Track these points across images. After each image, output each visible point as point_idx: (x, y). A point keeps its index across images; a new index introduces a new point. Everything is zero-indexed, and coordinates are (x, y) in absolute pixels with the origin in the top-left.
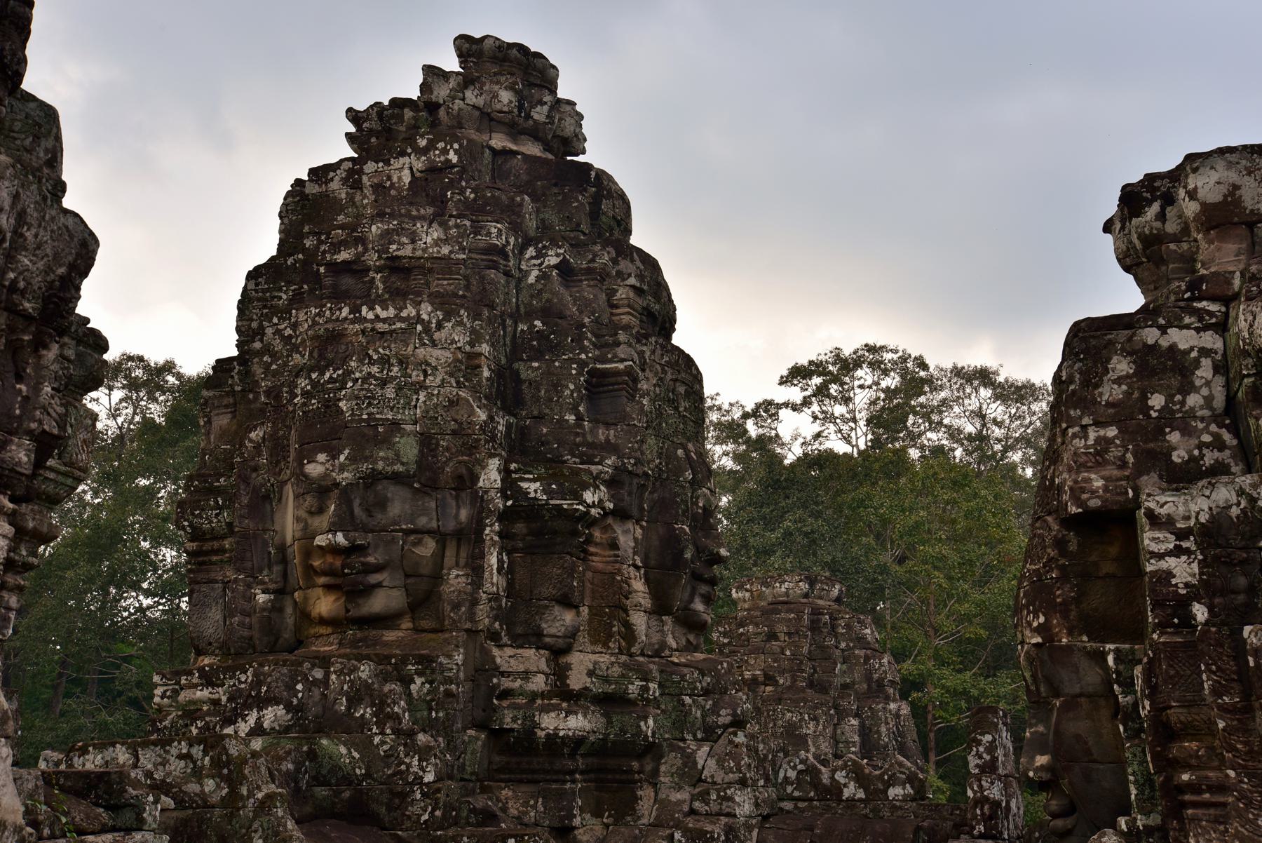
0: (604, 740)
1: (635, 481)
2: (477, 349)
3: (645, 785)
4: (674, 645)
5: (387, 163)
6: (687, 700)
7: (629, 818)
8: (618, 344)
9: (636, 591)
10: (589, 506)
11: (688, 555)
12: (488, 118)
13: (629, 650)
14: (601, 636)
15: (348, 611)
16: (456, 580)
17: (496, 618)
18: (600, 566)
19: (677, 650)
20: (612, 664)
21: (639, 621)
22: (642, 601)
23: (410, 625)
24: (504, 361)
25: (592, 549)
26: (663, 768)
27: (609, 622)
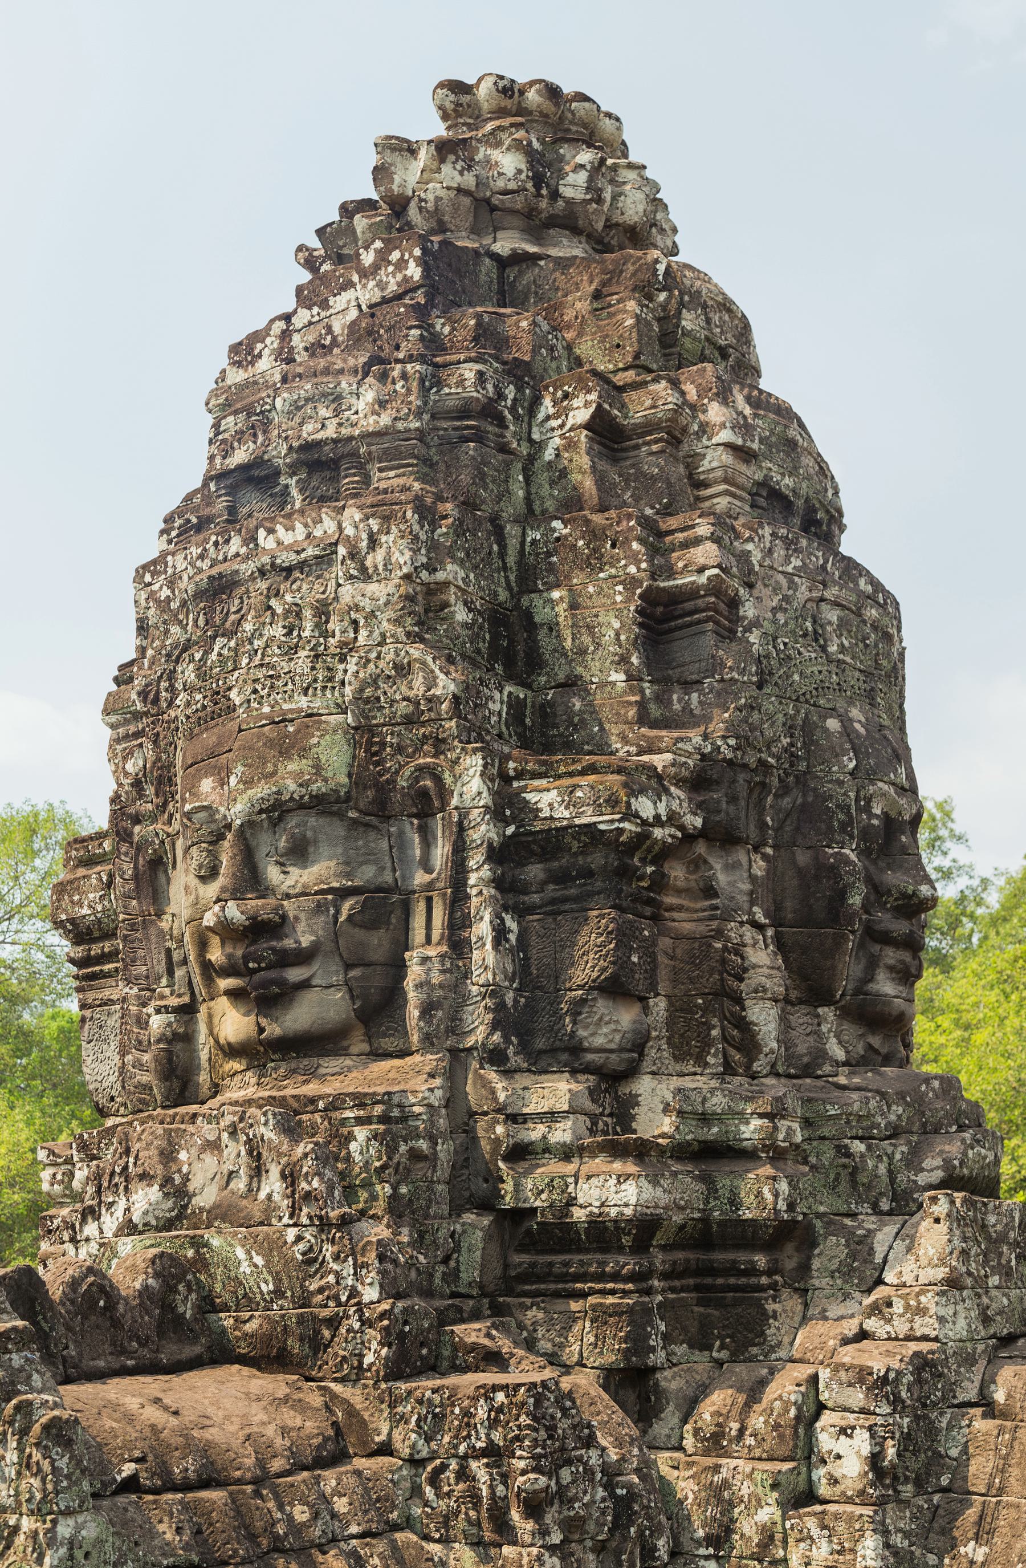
0: (705, 1220)
1: (742, 777)
2: (441, 576)
3: (785, 1293)
4: (840, 1055)
5: (325, 305)
6: (858, 1147)
7: (755, 1350)
8: (697, 541)
9: (755, 966)
10: (644, 822)
11: (856, 900)
12: (485, 208)
13: (748, 1067)
14: (688, 1047)
15: (261, 1030)
16: (421, 967)
17: (495, 1026)
18: (687, 926)
19: (844, 1064)
20: (712, 1091)
21: (765, 1018)
22: (768, 984)
23: (365, 1047)
24: (503, 595)
25: (670, 900)
26: (816, 1264)
27: (709, 1021)
